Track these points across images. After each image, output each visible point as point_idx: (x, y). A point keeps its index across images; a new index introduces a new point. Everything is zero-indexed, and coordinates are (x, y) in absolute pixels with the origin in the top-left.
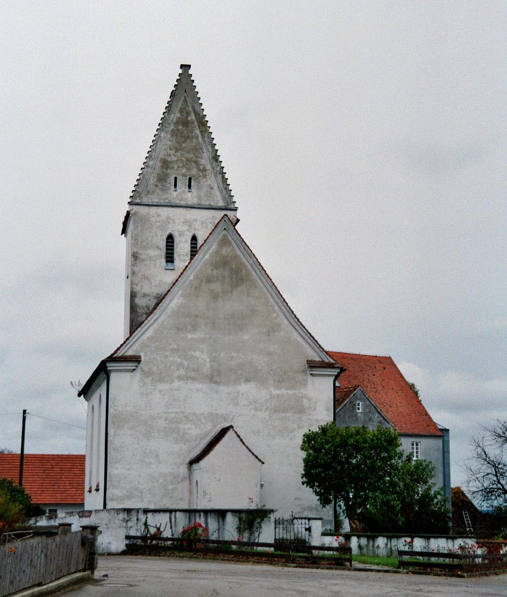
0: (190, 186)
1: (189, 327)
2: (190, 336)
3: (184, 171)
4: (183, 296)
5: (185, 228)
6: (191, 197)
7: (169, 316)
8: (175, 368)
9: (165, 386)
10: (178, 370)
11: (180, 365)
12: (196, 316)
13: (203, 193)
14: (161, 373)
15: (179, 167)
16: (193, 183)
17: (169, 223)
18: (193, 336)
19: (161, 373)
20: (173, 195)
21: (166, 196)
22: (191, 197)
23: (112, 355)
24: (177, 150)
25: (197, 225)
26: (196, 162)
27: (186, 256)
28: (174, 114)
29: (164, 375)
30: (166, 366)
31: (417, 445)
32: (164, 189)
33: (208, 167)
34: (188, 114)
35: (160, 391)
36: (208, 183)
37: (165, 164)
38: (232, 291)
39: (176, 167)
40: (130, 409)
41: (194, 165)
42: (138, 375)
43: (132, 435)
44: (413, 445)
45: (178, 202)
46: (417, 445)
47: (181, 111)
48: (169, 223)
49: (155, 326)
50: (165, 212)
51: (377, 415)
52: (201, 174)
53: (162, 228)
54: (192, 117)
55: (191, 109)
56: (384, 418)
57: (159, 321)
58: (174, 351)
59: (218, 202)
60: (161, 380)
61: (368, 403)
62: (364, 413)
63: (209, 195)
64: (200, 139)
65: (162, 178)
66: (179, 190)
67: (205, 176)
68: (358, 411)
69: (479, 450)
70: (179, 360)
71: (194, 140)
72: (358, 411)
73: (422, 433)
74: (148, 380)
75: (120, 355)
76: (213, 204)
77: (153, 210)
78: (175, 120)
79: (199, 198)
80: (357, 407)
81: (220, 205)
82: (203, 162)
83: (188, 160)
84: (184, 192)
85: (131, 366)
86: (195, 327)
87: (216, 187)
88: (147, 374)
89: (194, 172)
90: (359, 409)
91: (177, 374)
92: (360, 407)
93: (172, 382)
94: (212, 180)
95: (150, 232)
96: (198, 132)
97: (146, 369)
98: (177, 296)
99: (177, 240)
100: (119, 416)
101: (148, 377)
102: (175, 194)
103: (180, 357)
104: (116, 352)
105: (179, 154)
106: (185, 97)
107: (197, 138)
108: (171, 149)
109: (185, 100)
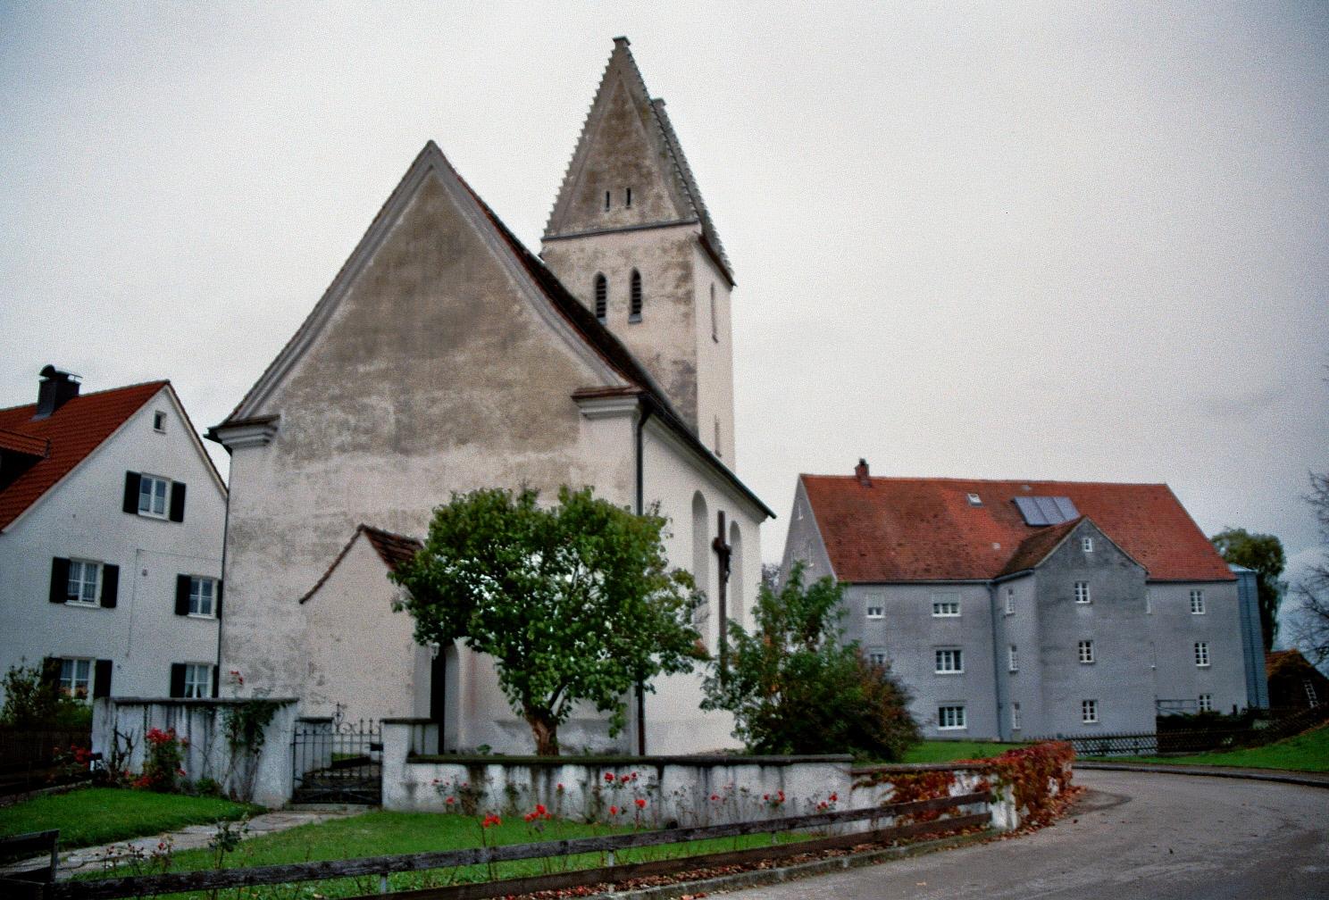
0: (629, 202)
1: (361, 353)
2: (361, 369)
3: (619, 181)
4: (354, 298)
5: (621, 261)
6: (630, 217)
7: (330, 338)
8: (334, 431)
9: (317, 467)
10: (340, 434)
11: (344, 425)
12: (376, 331)
13: (647, 208)
14: (311, 443)
15: (612, 177)
16: (633, 196)
17: (597, 257)
18: (368, 368)
19: (311, 443)
20: (605, 218)
21: (594, 221)
22: (630, 217)
23: (231, 417)
24: (609, 154)
25: (638, 255)
26: (637, 166)
27: (624, 303)
28: (605, 106)
29: (315, 447)
30: (319, 430)
31: (1199, 594)
32: (593, 213)
33: (655, 169)
34: (624, 102)
35: (308, 477)
36: (655, 191)
37: (594, 177)
38: (439, 275)
39: (608, 177)
40: (259, 513)
41: (635, 170)
42: (274, 450)
43: (260, 561)
44: (1192, 594)
45: (610, 226)
46: (1199, 594)
47: (615, 101)
48: (597, 257)
49: (305, 359)
50: (591, 244)
51: (1117, 555)
52: (644, 180)
53: (588, 267)
54: (630, 105)
55: (628, 94)
56: (1129, 559)
57: (312, 350)
58: (334, 399)
59: (670, 216)
60: (311, 456)
61: (1101, 538)
62: (1096, 553)
63: (657, 208)
64: (642, 132)
65: (589, 198)
66: (613, 209)
67: (650, 183)
68: (1086, 551)
69: (1307, 598)
70: (343, 415)
71: (634, 135)
72: (1086, 551)
73: (1206, 578)
74: (289, 459)
75: (244, 417)
76: (663, 220)
77: (575, 244)
78: (606, 114)
79: (642, 215)
80: (1085, 545)
81: (673, 219)
82: (648, 162)
83: (625, 165)
84: (620, 210)
85: (256, 434)
86: (371, 352)
87: (666, 194)
88: (288, 448)
89: (634, 180)
90: (1087, 548)
91: (337, 441)
92: (1090, 545)
93: (328, 456)
94: (662, 187)
95: (569, 276)
96: (639, 124)
97: (287, 437)
98: (345, 298)
99: (609, 281)
100: (241, 527)
101: (288, 452)
102: (606, 216)
103: (343, 409)
104: (236, 412)
105: (612, 159)
106: (620, 81)
107: (637, 132)
108: (600, 154)
109: (621, 85)
